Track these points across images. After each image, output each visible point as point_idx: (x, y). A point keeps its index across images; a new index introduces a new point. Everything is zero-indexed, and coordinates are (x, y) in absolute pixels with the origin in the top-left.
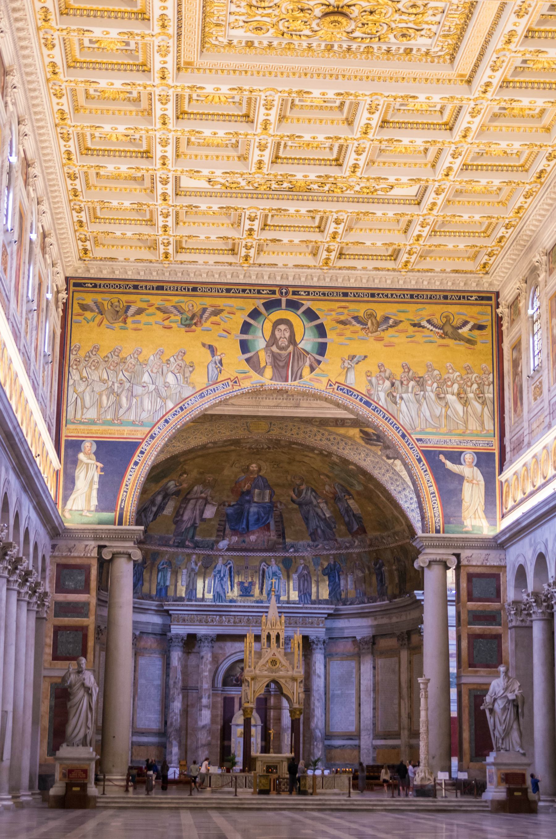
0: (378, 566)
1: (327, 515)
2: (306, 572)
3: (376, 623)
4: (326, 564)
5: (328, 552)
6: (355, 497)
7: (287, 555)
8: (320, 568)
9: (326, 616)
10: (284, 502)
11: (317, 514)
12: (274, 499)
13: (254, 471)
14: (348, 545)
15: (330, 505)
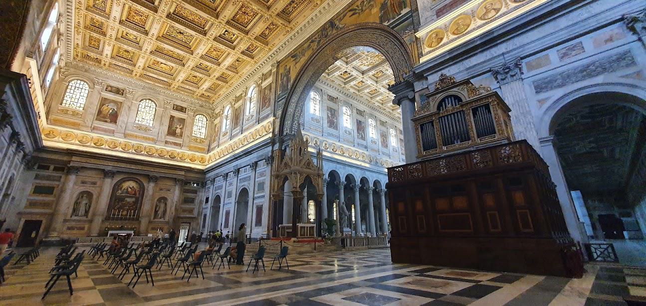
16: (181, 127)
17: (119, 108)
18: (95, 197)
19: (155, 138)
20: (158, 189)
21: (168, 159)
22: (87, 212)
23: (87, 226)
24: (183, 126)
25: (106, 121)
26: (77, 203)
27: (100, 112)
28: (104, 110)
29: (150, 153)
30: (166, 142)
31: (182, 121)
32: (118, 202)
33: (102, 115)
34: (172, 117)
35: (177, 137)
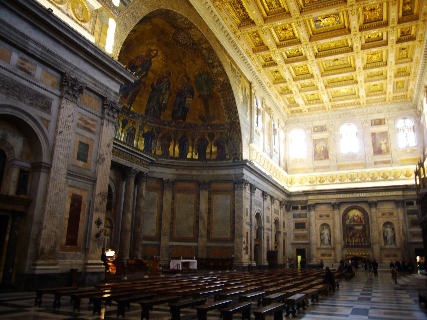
0: (182, 141)
1: (164, 102)
2: (133, 132)
3: (178, 172)
4: (146, 130)
5: (151, 124)
6: (195, 97)
7: (127, 117)
8: (142, 132)
9: (150, 162)
10: (146, 84)
11: (159, 99)
12: (142, 80)
13: (152, 55)
14: (166, 123)
15: (171, 96)
16: (385, 141)
17: (327, 144)
18: (331, 227)
19: (364, 162)
20: (380, 214)
21: (380, 181)
22: (330, 241)
23: (333, 253)
24: (387, 140)
25: (321, 159)
26: (321, 234)
27: (315, 153)
28: (318, 149)
29: (363, 179)
30: (375, 163)
31: (385, 134)
32: (350, 231)
33: (317, 155)
34: (373, 134)
35: (384, 153)
